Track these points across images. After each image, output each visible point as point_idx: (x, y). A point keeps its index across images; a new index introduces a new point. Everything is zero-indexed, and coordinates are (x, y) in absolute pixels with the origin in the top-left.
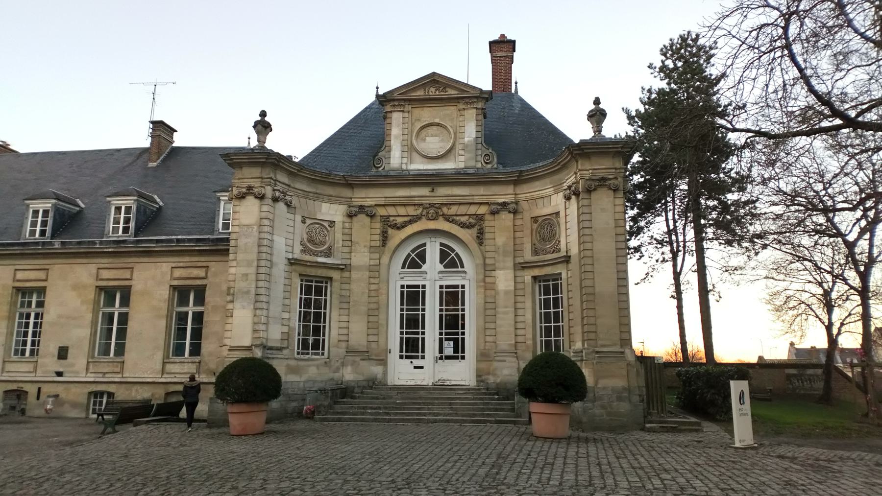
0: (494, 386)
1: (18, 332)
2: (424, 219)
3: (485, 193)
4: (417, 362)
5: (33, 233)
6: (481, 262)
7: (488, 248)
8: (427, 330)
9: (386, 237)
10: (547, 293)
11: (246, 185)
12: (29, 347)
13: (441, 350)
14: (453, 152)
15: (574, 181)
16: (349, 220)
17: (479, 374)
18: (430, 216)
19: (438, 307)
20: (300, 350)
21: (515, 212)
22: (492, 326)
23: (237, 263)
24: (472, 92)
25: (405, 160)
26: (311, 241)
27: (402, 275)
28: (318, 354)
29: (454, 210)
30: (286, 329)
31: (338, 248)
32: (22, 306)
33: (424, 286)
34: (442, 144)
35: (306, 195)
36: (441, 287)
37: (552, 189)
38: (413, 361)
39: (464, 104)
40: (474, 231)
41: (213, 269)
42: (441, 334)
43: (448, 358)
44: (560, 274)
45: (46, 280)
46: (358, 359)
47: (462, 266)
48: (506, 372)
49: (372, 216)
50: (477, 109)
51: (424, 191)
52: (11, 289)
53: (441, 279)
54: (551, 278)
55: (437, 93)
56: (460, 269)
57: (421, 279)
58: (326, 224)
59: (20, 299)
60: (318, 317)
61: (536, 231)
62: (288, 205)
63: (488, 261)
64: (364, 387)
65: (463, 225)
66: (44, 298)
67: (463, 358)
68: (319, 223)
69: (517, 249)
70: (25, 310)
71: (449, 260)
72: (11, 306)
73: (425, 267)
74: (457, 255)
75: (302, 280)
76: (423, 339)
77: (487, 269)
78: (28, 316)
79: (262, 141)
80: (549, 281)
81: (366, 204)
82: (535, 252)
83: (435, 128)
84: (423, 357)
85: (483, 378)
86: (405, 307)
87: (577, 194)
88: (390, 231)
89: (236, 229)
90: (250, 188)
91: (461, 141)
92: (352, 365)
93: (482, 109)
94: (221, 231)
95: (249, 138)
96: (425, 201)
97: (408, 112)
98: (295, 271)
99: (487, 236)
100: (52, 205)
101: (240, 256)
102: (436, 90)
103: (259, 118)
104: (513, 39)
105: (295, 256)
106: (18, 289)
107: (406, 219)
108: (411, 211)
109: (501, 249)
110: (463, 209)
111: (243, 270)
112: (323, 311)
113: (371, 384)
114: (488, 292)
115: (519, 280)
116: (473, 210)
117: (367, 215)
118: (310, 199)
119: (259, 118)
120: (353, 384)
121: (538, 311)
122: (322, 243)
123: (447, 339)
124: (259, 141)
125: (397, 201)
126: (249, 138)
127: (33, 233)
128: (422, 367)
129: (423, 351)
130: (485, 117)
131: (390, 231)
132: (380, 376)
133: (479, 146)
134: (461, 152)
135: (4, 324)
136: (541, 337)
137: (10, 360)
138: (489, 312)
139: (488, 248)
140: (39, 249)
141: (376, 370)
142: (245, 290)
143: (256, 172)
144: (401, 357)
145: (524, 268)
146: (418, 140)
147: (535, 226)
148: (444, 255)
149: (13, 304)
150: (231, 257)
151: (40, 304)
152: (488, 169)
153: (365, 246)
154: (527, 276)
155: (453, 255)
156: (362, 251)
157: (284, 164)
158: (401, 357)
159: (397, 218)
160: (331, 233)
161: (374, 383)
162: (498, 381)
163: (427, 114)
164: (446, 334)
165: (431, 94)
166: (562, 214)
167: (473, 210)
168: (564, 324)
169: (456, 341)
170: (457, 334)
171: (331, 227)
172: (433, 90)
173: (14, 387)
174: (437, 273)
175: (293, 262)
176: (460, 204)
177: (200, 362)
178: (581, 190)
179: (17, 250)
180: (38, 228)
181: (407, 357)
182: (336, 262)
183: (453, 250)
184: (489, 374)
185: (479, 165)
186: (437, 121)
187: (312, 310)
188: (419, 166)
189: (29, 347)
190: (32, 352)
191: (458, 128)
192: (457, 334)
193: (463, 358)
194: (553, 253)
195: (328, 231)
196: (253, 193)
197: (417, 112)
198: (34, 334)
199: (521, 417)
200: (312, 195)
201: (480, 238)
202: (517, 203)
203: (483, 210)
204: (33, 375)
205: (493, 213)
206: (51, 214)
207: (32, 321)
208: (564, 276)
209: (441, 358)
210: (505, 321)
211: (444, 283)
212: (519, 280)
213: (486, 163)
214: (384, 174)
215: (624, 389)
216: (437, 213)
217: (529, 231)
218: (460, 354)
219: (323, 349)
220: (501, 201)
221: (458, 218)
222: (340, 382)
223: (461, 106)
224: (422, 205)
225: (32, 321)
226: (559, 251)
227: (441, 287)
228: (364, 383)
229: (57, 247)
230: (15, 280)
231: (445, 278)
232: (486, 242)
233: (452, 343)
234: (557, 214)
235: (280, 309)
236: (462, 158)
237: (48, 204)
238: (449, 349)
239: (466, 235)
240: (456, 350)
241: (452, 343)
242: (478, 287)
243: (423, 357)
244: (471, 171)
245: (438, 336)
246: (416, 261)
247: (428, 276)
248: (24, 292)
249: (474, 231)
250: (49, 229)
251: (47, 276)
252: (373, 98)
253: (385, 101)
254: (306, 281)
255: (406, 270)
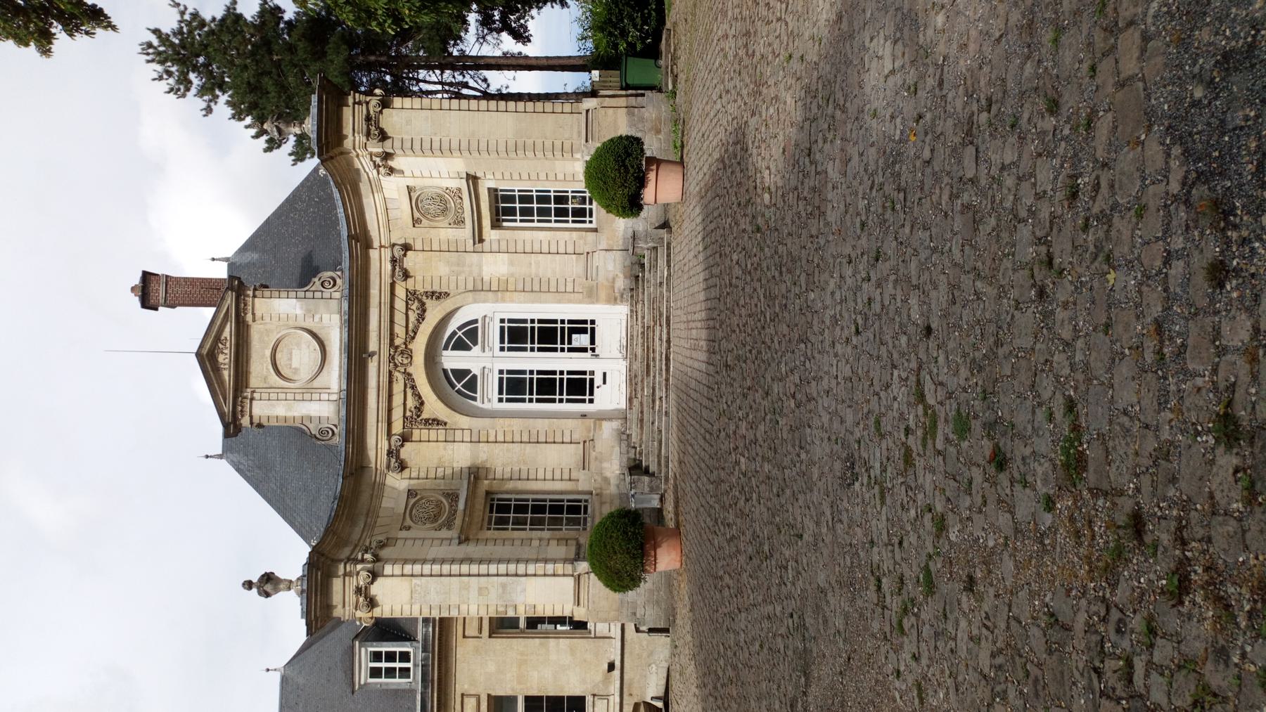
0: (628, 282)
2: (410, 370)
3: (378, 287)
4: (598, 380)
6: (470, 294)
7: (453, 286)
8: (558, 369)
9: (434, 420)
10: (512, 212)
11: (353, 598)
13: (584, 350)
14: (314, 330)
15: (368, 160)
16: (406, 473)
17: (613, 300)
18: (406, 361)
19: (528, 354)
20: (581, 528)
21: (406, 248)
22: (553, 284)
23: (464, 603)
24: (229, 302)
25: (325, 396)
26: (435, 518)
27: (486, 400)
28: (586, 507)
29: (400, 330)
30: (554, 543)
31: (445, 484)
33: (501, 372)
34: (304, 346)
35: (370, 527)
36: (502, 349)
37: (376, 195)
38: (596, 385)
39: (246, 314)
40: (429, 303)
41: (466, 687)
42: (563, 350)
43: (593, 341)
44: (489, 189)
46: (593, 454)
47: (476, 321)
48: (610, 267)
49: (405, 438)
50: (254, 296)
51: (372, 366)
53: (491, 349)
54: (494, 205)
55: (227, 351)
56: (479, 325)
57: (490, 375)
58: (412, 501)
60: (539, 509)
61: (431, 220)
62: (382, 545)
63: (470, 287)
64: (628, 446)
65: (421, 318)
67: (593, 322)
68: (409, 510)
69: (453, 249)
71: (468, 337)
73: (476, 371)
74: (460, 328)
75: (489, 529)
76: (569, 373)
77: (480, 289)
79: (289, 585)
80: (497, 208)
81: (386, 447)
82: (459, 222)
83: (278, 356)
84: (592, 373)
85: (617, 295)
86: (527, 397)
87: (387, 156)
88: (425, 416)
89: (416, 609)
90: (358, 590)
91: (301, 318)
92: (601, 462)
93: (255, 289)
94: (411, 680)
95: (268, 670)
96: (385, 369)
97: (253, 392)
98: (477, 534)
99: (436, 288)
101: (454, 600)
102: (222, 353)
103: (254, 590)
104: (140, 274)
105: (456, 535)
107: (409, 392)
108: (398, 387)
109: (455, 268)
110: (399, 318)
111: (474, 593)
112: (530, 503)
113: (624, 437)
114: (511, 287)
115: (495, 248)
116: (400, 305)
117: (402, 446)
118: (376, 522)
119: (254, 590)
120: (625, 460)
121: (536, 224)
122: (439, 505)
123: (570, 342)
124: (289, 589)
125: (383, 405)
126: (268, 670)
128: (605, 374)
129: (584, 373)
130: (266, 287)
131: (425, 416)
132: (615, 424)
133: (309, 294)
134: (317, 318)
136: (567, 222)
138: (536, 288)
139: (453, 286)
141: (608, 429)
142: (500, 590)
143: (337, 584)
144: (591, 401)
145: (481, 240)
146: (295, 378)
147: (424, 221)
148: (460, 346)
150: (454, 614)
152: (344, 283)
153: (445, 449)
154: (490, 234)
155: (460, 333)
156: (450, 452)
157: (316, 595)
158: (591, 401)
159: (409, 406)
160: (424, 494)
161: (623, 433)
162: (621, 276)
163: (259, 368)
164: (563, 343)
165: (227, 361)
166: (411, 182)
167: (400, 305)
168: (553, 188)
169: (573, 331)
170: (563, 329)
171: (416, 495)
172: (221, 358)
174: (484, 355)
175: (464, 539)
176: (392, 322)
177: (594, 695)
178: (380, 150)
181: (592, 393)
182: (465, 486)
183: (454, 333)
184: (613, 287)
185: (337, 295)
186: (268, 353)
187: (529, 515)
188: (334, 377)
191: (281, 323)
192: (563, 329)
193: (593, 322)
194: (461, 198)
195: (422, 498)
196: (366, 588)
197: (254, 381)
199: (663, 239)
200: (369, 520)
201: (438, 296)
202: (393, 245)
203: (400, 292)
205: (406, 275)
208: (492, 185)
209: (593, 350)
210: (549, 267)
211: (497, 345)
212: (495, 248)
213: (334, 285)
214: (343, 426)
215: (628, 114)
216: (402, 353)
217: (432, 231)
218: (589, 326)
219: (580, 501)
220: (389, 267)
221: (411, 326)
222: (622, 477)
223: (249, 317)
224: (390, 372)
226: (459, 190)
227: (502, 349)
228: (624, 445)
231: (491, 345)
232: (444, 289)
233: (574, 336)
234: (410, 190)
235: (527, 548)
236: (326, 317)
238: (581, 340)
239: (434, 313)
240: (584, 331)
241: (574, 336)
242: (503, 301)
243: (592, 373)
244: (345, 305)
245: (566, 354)
246: (468, 382)
247: (488, 365)
249: (429, 303)
252: (224, 463)
253: (235, 426)
254: (490, 523)
255: (478, 395)
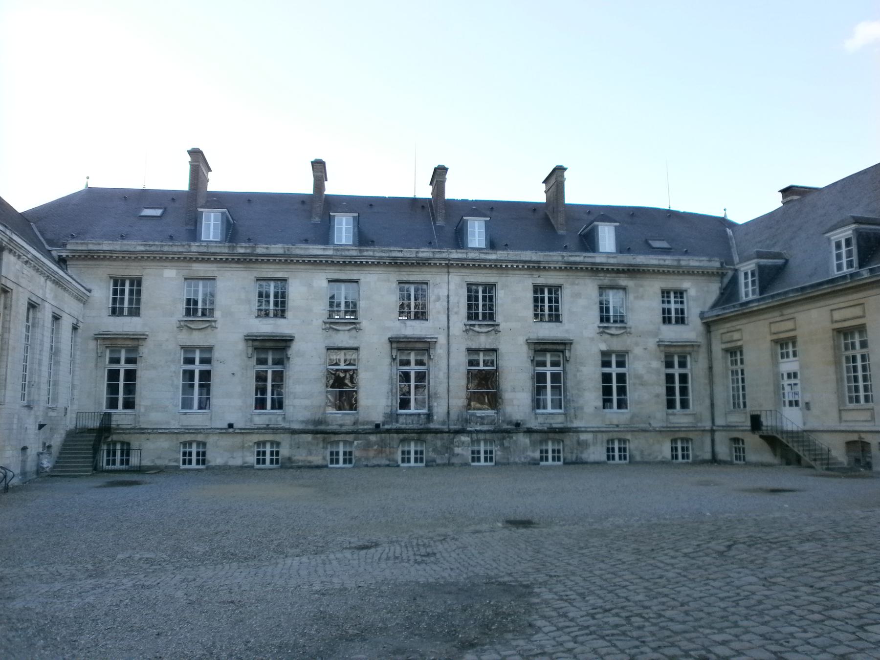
1: (849, 378)
5: (839, 267)
12: (862, 394)
32: (846, 349)
45: (863, 317)
52: (831, 332)
59: (843, 342)
66: (867, 337)
70: (850, 353)
72: (835, 349)
78: (854, 358)
100: (853, 231)
106: (839, 331)
127: (839, 267)
135: (831, 369)
137: (846, 408)
140: (849, 283)
149: (836, 348)
151: (864, 345)
173: (855, 437)
179: (827, 288)
180: (844, 260)
189: (862, 394)
190: (867, 399)
198: (865, 378)
204: (872, 424)
206: (854, 242)
207: (859, 363)
225: (859, 363)
229: (866, 276)
230: (833, 322)
237: (847, 232)
248: (844, 332)
250: (855, 258)
251: (864, 312)
